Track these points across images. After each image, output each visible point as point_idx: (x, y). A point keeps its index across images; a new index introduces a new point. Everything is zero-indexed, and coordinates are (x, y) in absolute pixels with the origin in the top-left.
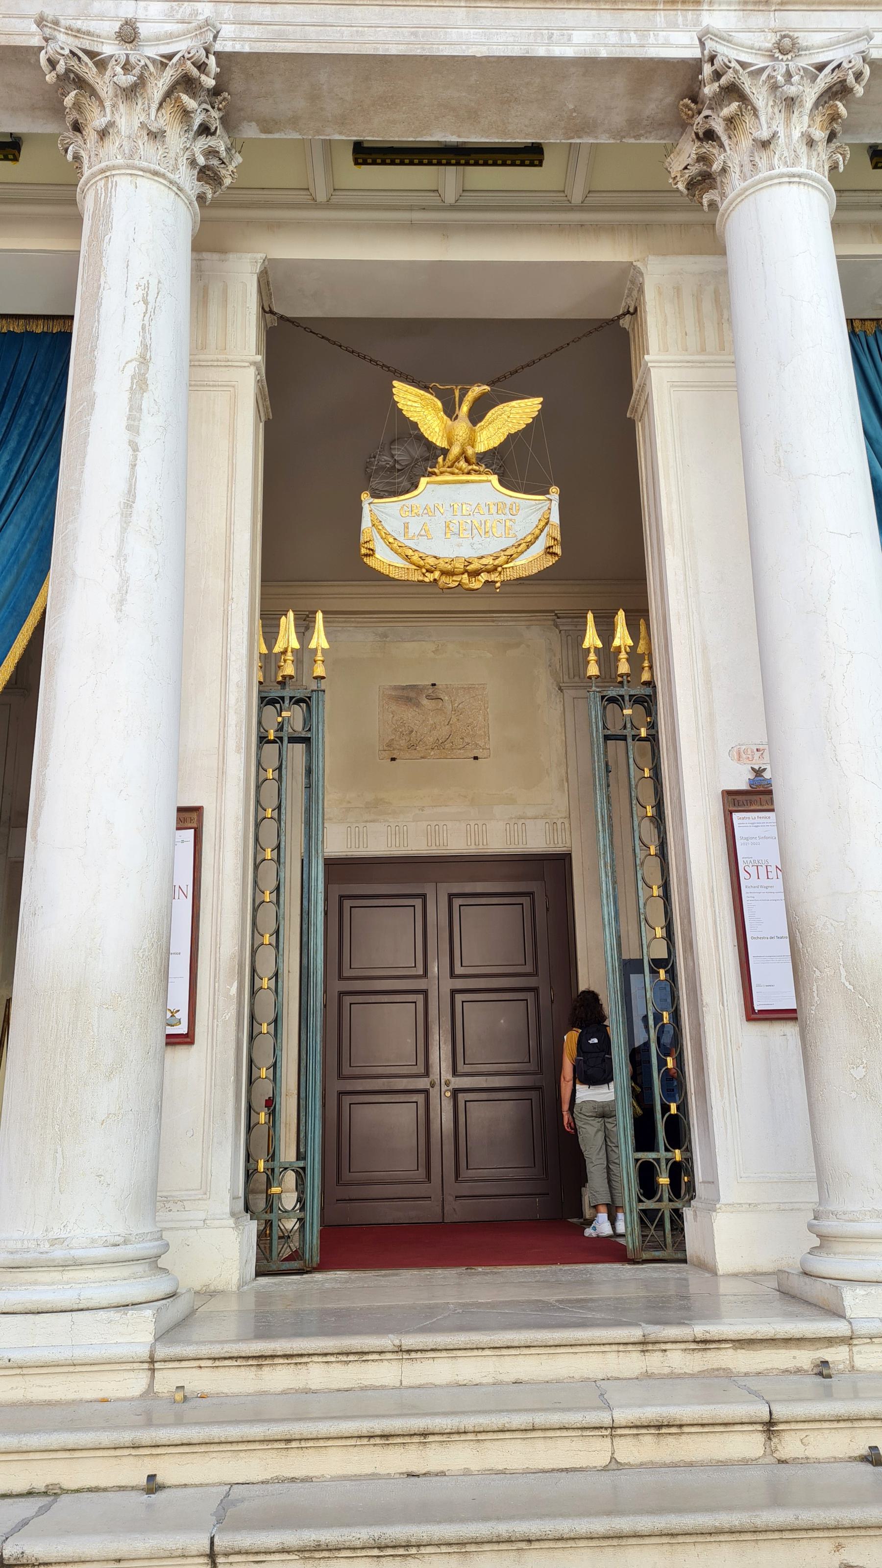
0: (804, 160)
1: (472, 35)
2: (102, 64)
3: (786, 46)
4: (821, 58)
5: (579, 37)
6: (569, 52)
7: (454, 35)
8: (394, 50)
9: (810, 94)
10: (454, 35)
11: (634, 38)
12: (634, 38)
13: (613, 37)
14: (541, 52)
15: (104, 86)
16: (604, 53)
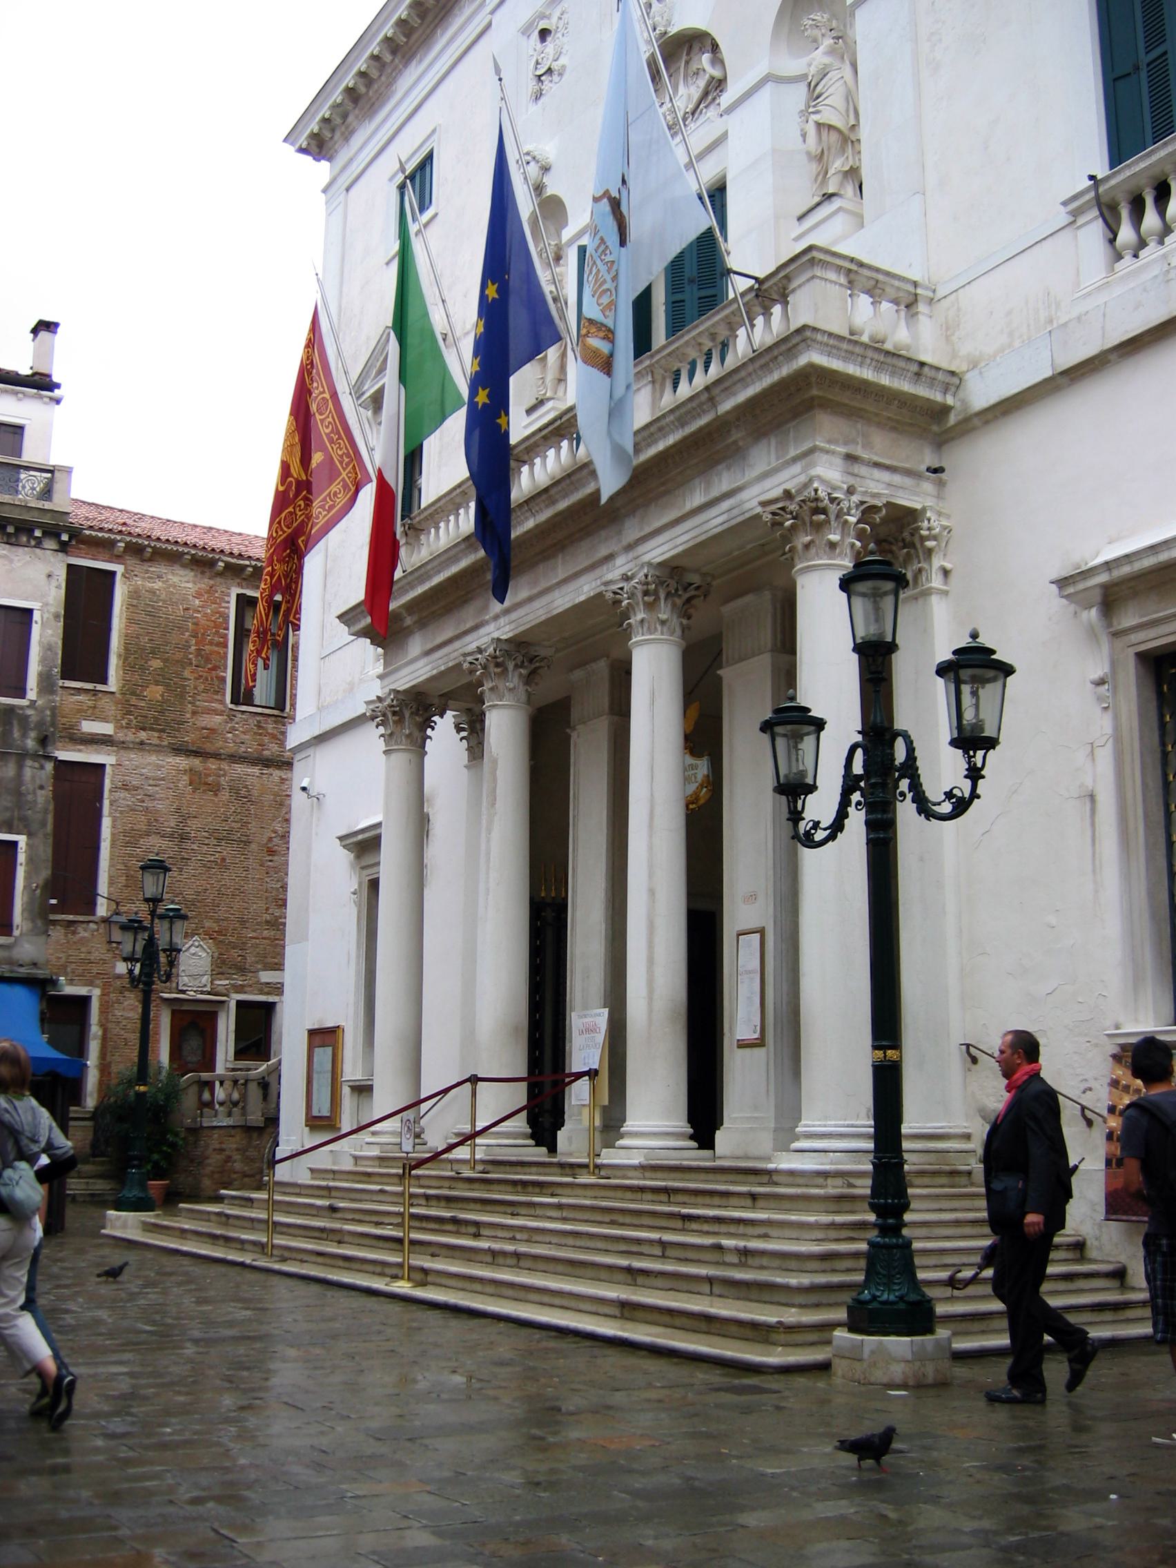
5: (586, 588)
6: (582, 598)
7: (557, 603)
14: (577, 601)
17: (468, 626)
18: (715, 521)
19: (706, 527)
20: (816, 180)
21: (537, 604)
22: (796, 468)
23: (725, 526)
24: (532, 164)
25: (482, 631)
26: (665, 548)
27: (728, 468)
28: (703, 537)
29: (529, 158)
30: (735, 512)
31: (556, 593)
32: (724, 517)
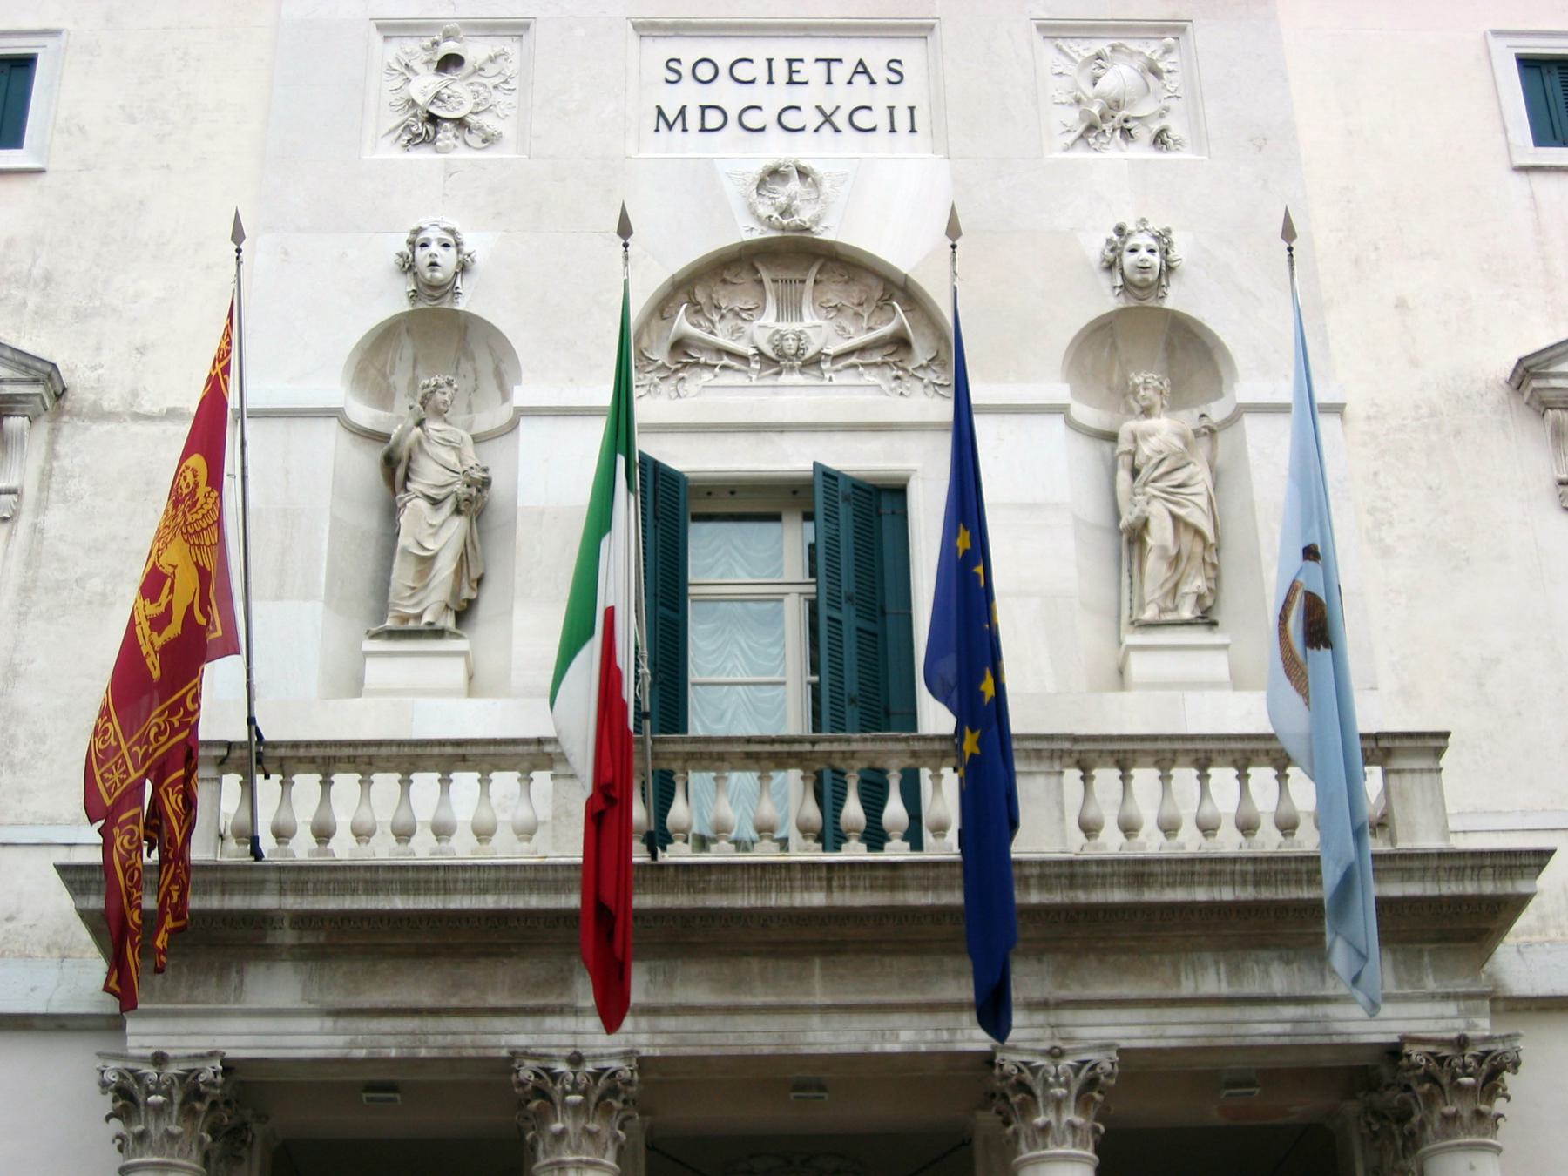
0: (1069, 1138)
1: (825, 1037)
2: (555, 1077)
3: (1055, 1054)
4: (1084, 1057)
6: (895, 1048)
7: (810, 1037)
8: (766, 1050)
9: (1075, 1088)
10: (810, 1037)
11: (945, 1035)
12: (945, 1035)
13: (930, 1035)
14: (876, 1048)
15: (557, 1098)
16: (923, 1048)
17: (492, 1000)
18: (1266, 1027)
19: (1242, 1030)
20: (1162, 586)
21: (775, 1023)
22: (1451, 1008)
23: (1285, 1040)
24: (453, 250)
25: (570, 1023)
26: (1136, 1031)
27: (1288, 962)
28: (1232, 1042)
29: (451, 240)
30: (1312, 1027)
31: (815, 1020)
32: (1288, 1027)
